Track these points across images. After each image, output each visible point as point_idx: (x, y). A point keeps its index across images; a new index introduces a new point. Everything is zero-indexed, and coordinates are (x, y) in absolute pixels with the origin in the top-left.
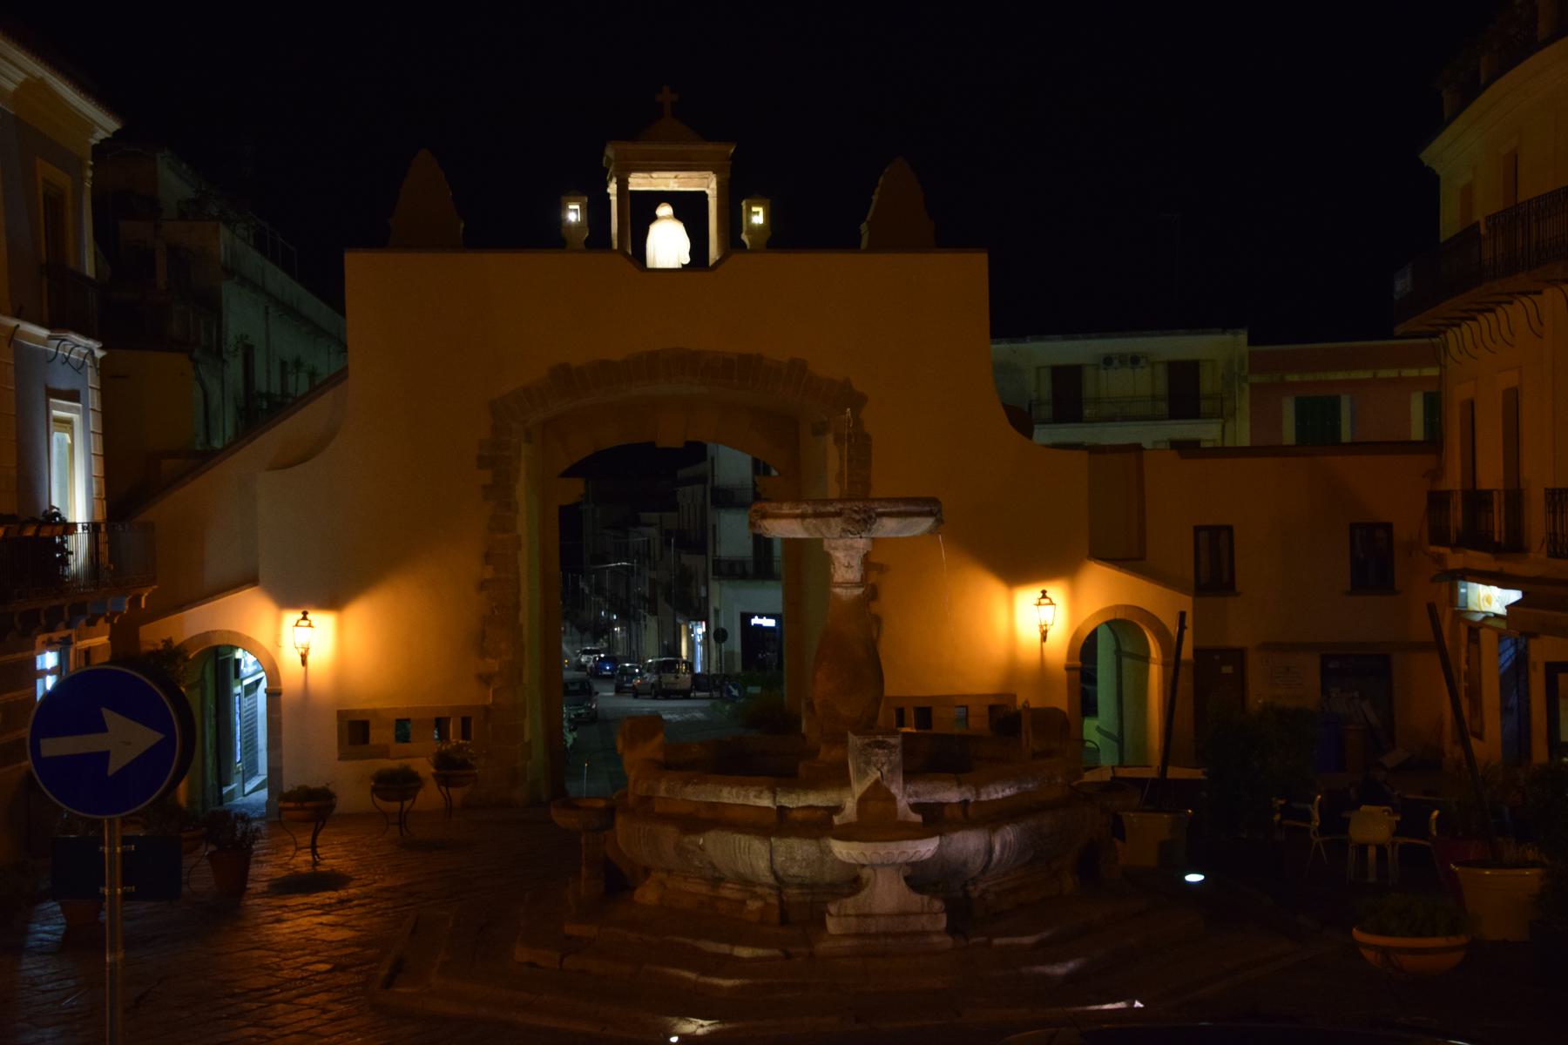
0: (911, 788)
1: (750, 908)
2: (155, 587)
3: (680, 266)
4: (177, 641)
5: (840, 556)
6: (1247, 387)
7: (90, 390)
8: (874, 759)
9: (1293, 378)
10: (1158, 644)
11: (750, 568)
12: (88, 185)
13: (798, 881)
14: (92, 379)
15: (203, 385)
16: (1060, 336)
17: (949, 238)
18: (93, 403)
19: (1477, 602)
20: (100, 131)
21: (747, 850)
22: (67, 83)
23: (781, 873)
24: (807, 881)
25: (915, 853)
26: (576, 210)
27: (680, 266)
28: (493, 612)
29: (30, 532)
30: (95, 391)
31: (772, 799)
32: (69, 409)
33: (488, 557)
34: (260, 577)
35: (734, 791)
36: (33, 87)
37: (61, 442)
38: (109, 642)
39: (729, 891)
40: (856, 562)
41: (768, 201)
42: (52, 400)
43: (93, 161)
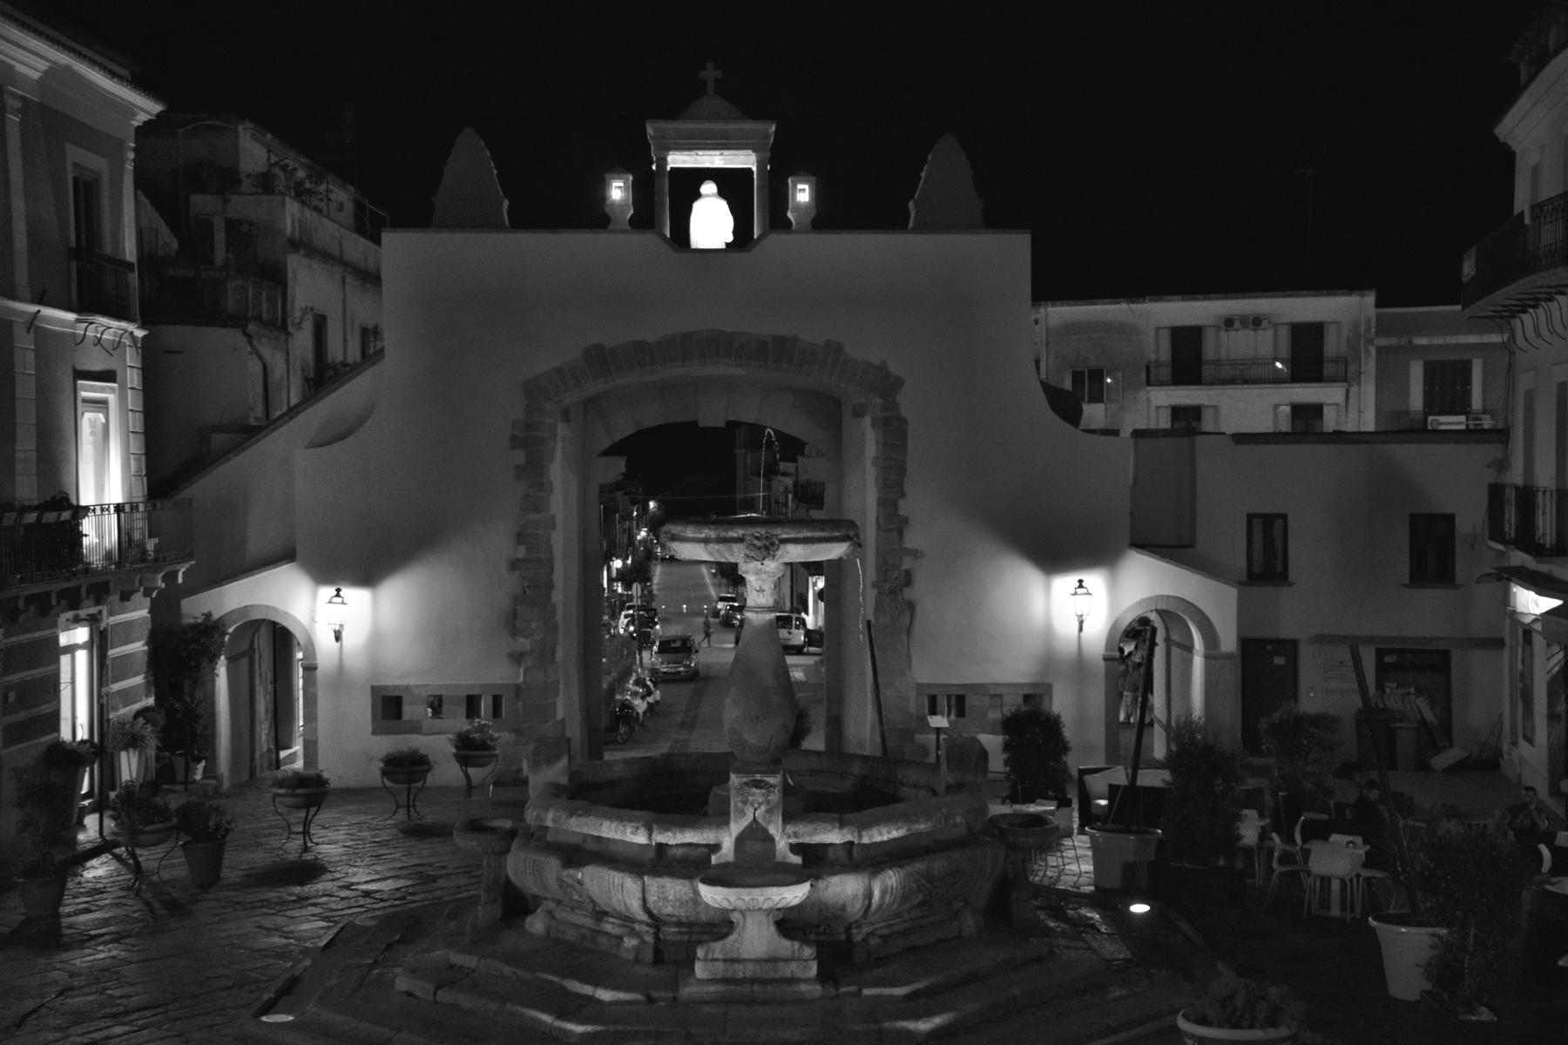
0: (790, 829)
1: (625, 945)
2: (193, 562)
3: (724, 247)
4: (216, 616)
5: (751, 579)
6: (1373, 350)
7: (128, 369)
8: (750, 798)
9: (1422, 341)
10: (1200, 637)
12: (129, 167)
13: (674, 919)
14: (132, 358)
15: (261, 358)
16: (1180, 297)
17: (995, 220)
18: (132, 382)
19: (1526, 604)
20: (142, 113)
21: (620, 888)
22: (97, 69)
23: (655, 912)
24: (684, 920)
25: (780, 900)
26: (620, 187)
27: (724, 247)
28: (525, 592)
29: (31, 517)
30: (135, 370)
31: (647, 836)
32: (102, 390)
33: (520, 538)
34: (297, 555)
35: (613, 825)
36: (55, 73)
37: (92, 424)
38: (149, 615)
39: (608, 927)
40: (768, 586)
41: (814, 178)
42: (80, 382)
43: (136, 143)
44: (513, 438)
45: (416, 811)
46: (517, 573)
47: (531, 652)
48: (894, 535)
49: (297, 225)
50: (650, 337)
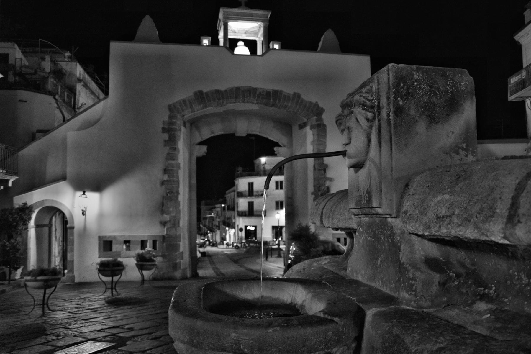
11: (247, 213)
28: (167, 195)
33: (165, 171)
41: (280, 43)
44: (164, 130)
45: (116, 292)
46: (164, 187)
47: (170, 221)
48: (322, 172)
49: (82, 76)
50: (223, 88)
